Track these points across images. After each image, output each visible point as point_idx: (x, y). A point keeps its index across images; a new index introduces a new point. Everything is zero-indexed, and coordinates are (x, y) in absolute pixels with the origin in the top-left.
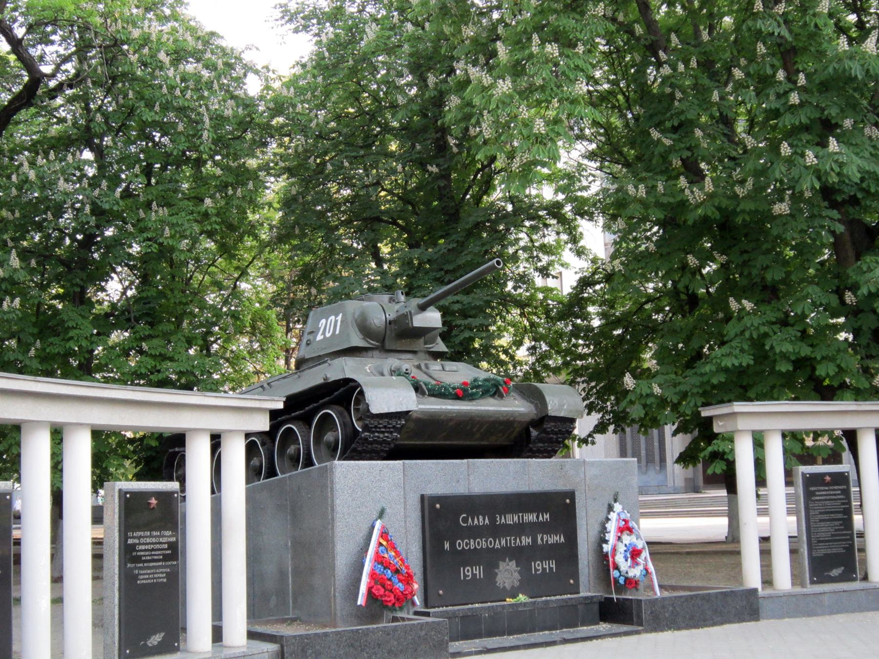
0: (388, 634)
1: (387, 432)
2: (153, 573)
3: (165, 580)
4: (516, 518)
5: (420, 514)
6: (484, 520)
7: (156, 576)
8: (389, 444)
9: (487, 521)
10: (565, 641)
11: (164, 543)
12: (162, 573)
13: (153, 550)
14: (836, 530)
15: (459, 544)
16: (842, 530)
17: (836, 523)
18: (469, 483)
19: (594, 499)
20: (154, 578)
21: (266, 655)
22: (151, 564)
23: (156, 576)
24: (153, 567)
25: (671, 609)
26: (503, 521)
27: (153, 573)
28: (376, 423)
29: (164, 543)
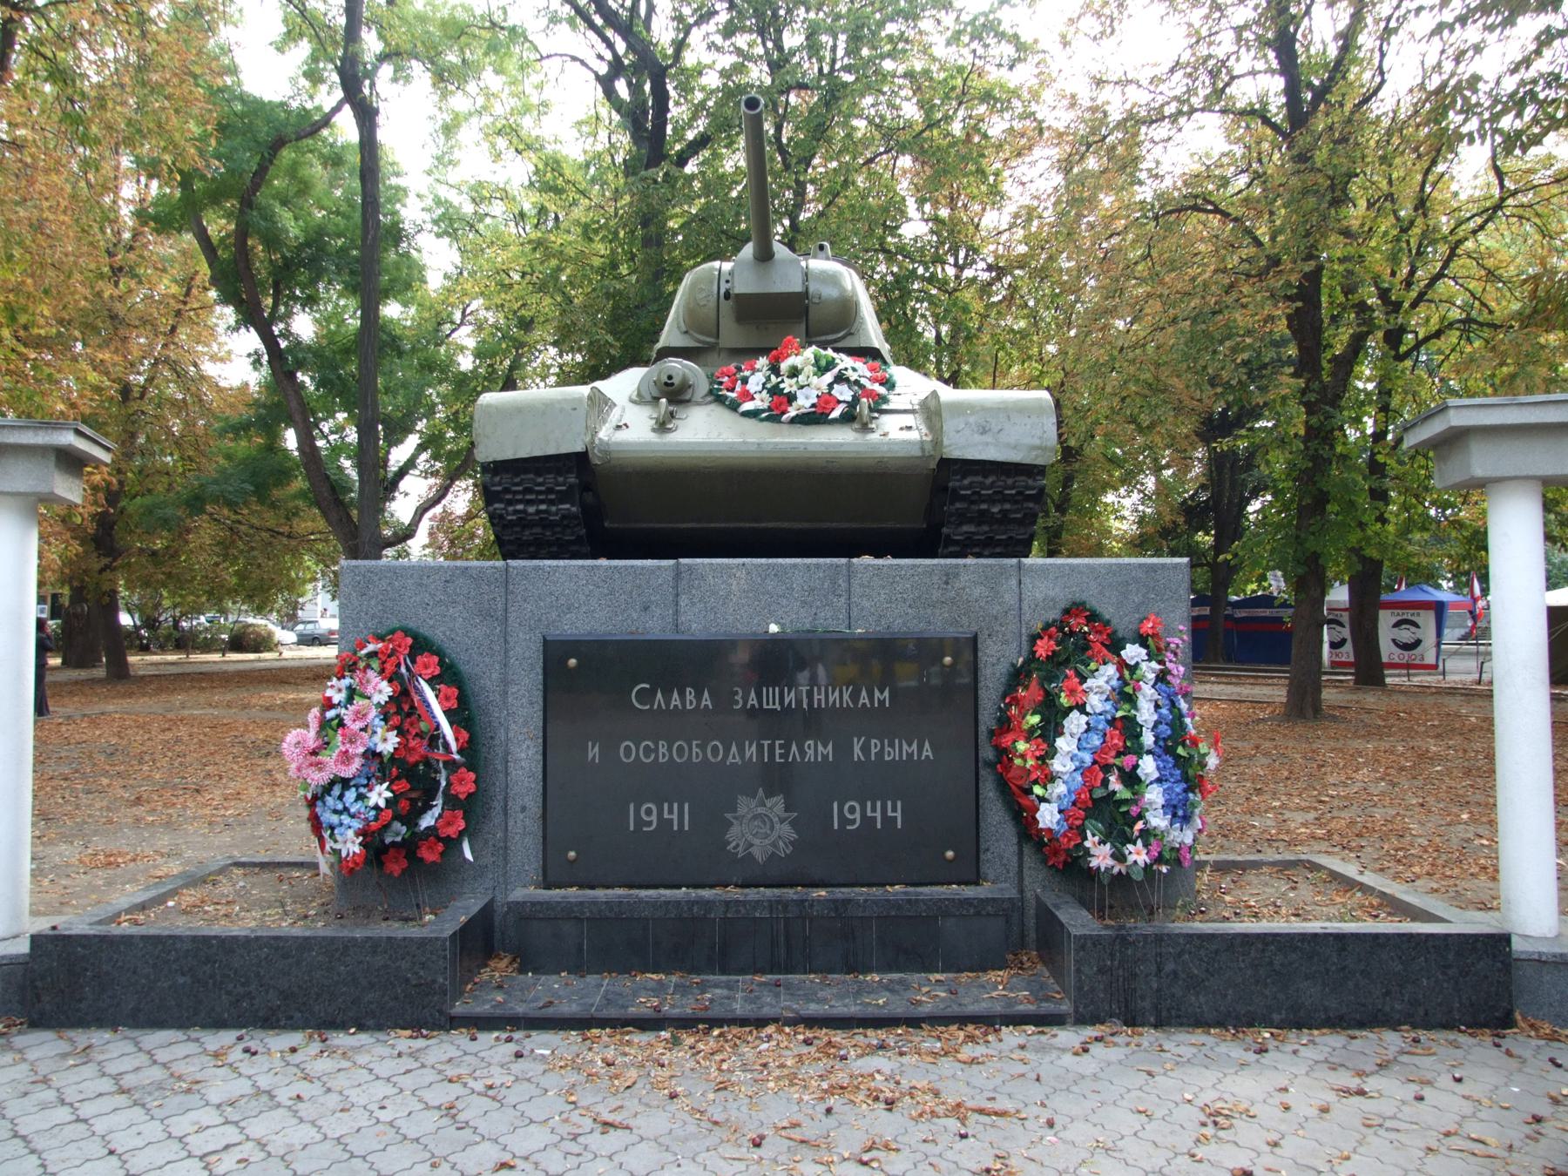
0: (285, 956)
6: (699, 696)
9: (706, 700)
15: (628, 750)
18: (676, 612)
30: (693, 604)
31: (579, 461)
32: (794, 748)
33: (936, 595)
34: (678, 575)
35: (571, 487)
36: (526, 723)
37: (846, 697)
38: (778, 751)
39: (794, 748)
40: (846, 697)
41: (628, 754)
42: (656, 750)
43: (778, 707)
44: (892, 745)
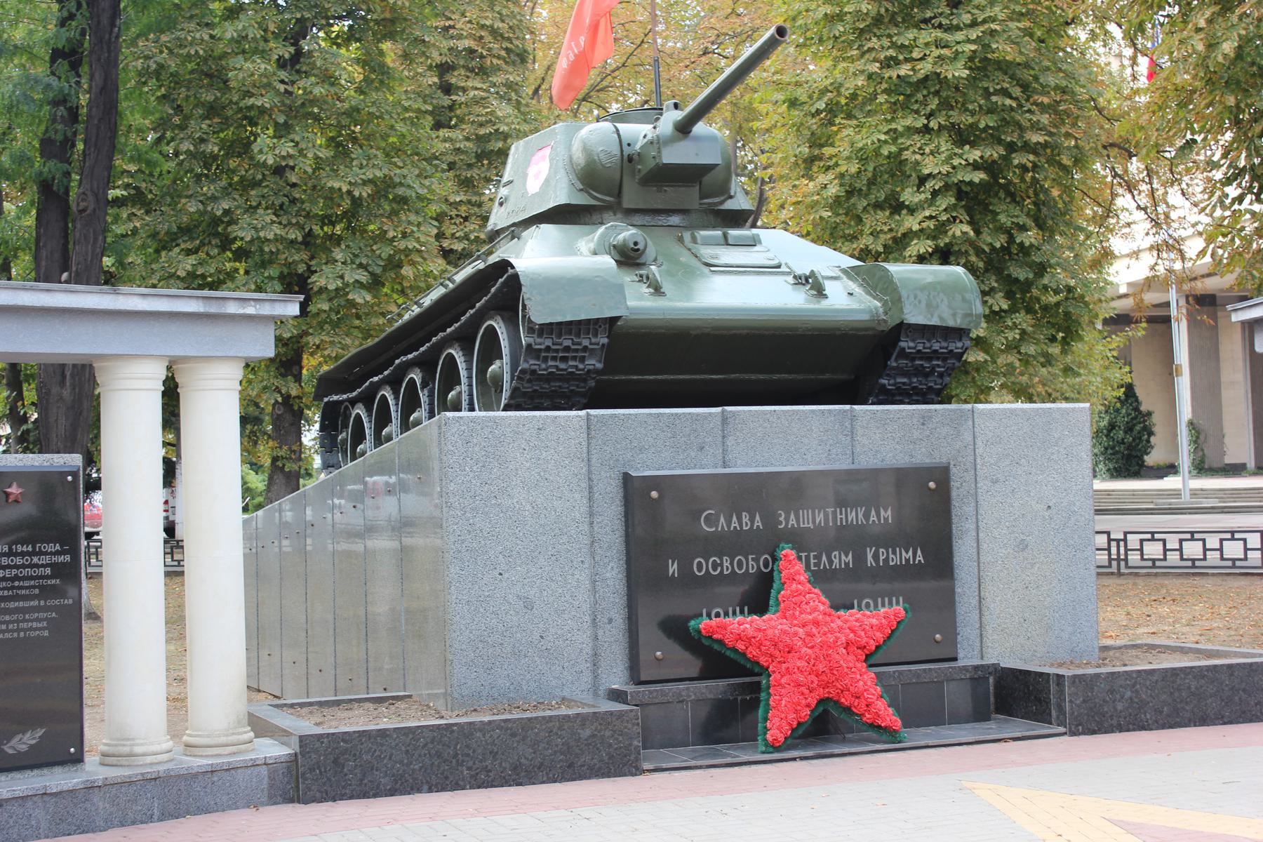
0: (513, 735)
1: (574, 358)
2: (18, 621)
3: (46, 633)
5: (621, 509)
6: (752, 520)
7: (25, 625)
8: (585, 381)
9: (758, 522)
11: (43, 566)
12: (38, 620)
13: (16, 578)
15: (700, 566)
19: (995, 482)
20: (18, 630)
21: (264, 771)
22: (12, 605)
23: (25, 625)
24: (16, 610)
25: (1128, 694)
26: (792, 521)
27: (18, 621)
28: (548, 343)
29: (43, 566)
30: (738, 444)
31: (613, 320)
32: (824, 558)
33: (916, 434)
34: (725, 419)
36: (610, 547)
37: (860, 516)
38: (812, 561)
39: (824, 558)
40: (860, 516)
41: (700, 569)
42: (721, 565)
43: (811, 525)
44: (894, 553)
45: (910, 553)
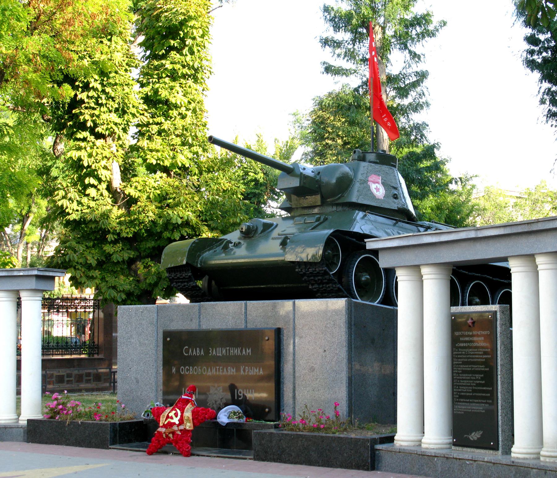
4: (224, 351)
6: (200, 351)
9: (202, 353)
10: (218, 457)
14: (478, 385)
15: (182, 369)
16: (483, 385)
17: (478, 376)
26: (214, 353)
35: (190, 276)
41: (182, 371)
42: (189, 370)
45: (258, 370)
